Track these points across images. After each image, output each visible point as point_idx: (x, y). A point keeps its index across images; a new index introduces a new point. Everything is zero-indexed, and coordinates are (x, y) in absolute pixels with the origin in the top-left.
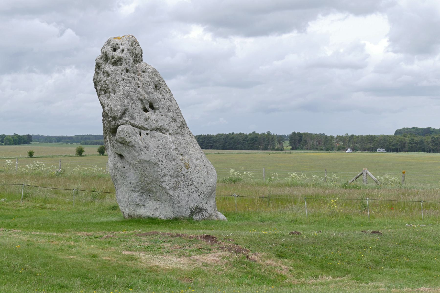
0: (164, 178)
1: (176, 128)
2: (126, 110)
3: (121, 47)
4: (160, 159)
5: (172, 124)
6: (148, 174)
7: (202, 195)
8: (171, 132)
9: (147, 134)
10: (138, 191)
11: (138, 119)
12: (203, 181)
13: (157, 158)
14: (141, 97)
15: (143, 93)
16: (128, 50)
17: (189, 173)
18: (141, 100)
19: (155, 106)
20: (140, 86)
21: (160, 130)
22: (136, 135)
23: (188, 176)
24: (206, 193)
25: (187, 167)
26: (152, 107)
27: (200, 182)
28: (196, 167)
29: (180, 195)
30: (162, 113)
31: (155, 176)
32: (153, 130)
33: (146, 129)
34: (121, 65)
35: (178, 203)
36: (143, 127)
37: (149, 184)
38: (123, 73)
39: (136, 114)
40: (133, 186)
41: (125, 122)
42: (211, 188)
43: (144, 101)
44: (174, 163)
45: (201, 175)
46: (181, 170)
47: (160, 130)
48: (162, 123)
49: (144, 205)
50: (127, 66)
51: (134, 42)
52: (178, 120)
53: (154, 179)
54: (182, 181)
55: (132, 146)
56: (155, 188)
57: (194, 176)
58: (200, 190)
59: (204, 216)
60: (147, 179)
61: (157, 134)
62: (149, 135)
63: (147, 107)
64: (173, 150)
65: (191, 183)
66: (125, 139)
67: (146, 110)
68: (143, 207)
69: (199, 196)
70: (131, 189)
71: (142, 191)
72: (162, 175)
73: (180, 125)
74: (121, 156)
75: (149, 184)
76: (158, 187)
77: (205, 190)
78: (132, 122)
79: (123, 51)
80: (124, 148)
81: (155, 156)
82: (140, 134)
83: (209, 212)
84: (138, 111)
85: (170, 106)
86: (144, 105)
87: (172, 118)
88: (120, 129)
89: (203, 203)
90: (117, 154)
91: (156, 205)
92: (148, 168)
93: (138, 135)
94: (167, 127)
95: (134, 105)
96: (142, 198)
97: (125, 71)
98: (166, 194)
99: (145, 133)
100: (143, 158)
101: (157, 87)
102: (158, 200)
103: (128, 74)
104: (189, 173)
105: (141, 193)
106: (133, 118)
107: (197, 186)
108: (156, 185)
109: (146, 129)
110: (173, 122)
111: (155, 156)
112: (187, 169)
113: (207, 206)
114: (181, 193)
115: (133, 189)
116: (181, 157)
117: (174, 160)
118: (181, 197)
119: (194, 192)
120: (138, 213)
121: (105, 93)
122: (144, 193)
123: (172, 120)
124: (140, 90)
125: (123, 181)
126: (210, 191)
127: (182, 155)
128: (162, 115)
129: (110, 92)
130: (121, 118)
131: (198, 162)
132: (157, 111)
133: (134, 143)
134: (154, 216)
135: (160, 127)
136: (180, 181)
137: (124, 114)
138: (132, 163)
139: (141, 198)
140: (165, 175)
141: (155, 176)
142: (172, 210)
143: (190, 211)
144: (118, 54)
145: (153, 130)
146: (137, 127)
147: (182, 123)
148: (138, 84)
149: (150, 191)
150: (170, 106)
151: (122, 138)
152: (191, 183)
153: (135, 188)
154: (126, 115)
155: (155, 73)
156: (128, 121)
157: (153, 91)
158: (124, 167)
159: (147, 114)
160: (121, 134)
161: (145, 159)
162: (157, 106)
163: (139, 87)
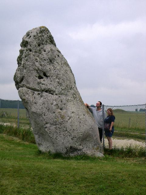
1: (61, 90)
2: (23, 77)
7: (75, 139)
9: (39, 94)
11: (32, 83)
12: (75, 128)
14: (37, 68)
17: (64, 122)
18: (37, 71)
21: (48, 91)
23: (63, 124)
24: (77, 137)
25: (63, 117)
26: (45, 75)
27: (72, 129)
32: (43, 91)
33: (38, 91)
39: (31, 79)
42: (82, 134)
43: (39, 71)
44: (54, 114)
45: (73, 124)
46: (58, 120)
47: (48, 91)
48: (50, 87)
51: (44, 31)
54: (59, 128)
57: (68, 125)
58: (72, 135)
63: (42, 75)
65: (65, 129)
67: (40, 77)
69: (72, 139)
71: (39, 134)
72: (44, 123)
77: (77, 135)
78: (28, 85)
79: (30, 37)
86: (39, 74)
89: (77, 145)
94: (53, 89)
95: (30, 73)
96: (40, 139)
101: (51, 61)
106: (28, 82)
107: (70, 132)
109: (38, 91)
113: (81, 147)
116: (60, 110)
117: (54, 113)
118: (59, 139)
123: (58, 84)
127: (61, 109)
131: (72, 115)
133: (27, 100)
135: (49, 89)
140: (47, 123)
145: (43, 91)
146: (31, 89)
147: (67, 87)
148: (36, 59)
150: (58, 75)
154: (23, 81)
156: (24, 85)
159: (42, 80)
162: (48, 75)
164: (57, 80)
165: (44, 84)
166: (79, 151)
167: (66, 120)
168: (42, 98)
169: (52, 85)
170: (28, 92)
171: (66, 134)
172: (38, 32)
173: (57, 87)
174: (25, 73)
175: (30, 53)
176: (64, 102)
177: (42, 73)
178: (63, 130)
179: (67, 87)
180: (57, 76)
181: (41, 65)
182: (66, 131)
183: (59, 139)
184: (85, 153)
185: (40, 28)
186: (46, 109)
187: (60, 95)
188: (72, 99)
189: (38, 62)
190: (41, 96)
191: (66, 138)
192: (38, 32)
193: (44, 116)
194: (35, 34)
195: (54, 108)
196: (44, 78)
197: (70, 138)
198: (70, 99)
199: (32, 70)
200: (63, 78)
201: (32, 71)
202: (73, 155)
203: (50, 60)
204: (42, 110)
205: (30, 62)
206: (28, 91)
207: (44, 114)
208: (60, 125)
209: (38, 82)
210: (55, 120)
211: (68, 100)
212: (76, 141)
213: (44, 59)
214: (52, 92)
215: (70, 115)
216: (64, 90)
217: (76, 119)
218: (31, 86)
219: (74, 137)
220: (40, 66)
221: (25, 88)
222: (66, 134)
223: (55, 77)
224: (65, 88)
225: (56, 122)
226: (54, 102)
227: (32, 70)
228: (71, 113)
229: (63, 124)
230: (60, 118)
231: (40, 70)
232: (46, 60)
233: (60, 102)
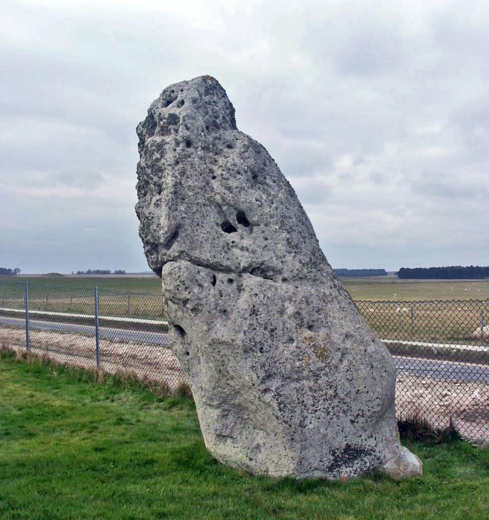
0: (268, 383)
1: (298, 265)
4: (258, 340)
5: (289, 258)
7: (361, 420)
9: (231, 281)
10: (218, 407)
11: (207, 246)
16: (194, 101)
17: (327, 369)
20: (215, 175)
24: (368, 414)
26: (243, 219)
27: (353, 390)
28: (343, 355)
29: (307, 422)
33: (228, 270)
36: (221, 266)
37: (238, 392)
40: (207, 395)
41: (177, 254)
42: (380, 402)
43: (225, 208)
45: (355, 375)
49: (231, 437)
50: (188, 133)
58: (354, 408)
59: (368, 464)
60: (232, 383)
62: (235, 284)
63: (233, 220)
64: (289, 318)
65: (331, 392)
67: (229, 228)
69: (352, 422)
70: (204, 400)
71: (226, 407)
73: (307, 259)
75: (238, 392)
77: (366, 408)
78: (196, 254)
79: (182, 103)
81: (245, 332)
83: (378, 455)
85: (286, 217)
86: (225, 216)
87: (289, 243)
88: (166, 269)
89: (363, 437)
94: (276, 263)
98: (274, 418)
99: (225, 279)
100: (219, 335)
104: (327, 369)
107: (348, 400)
108: (253, 398)
109: (228, 270)
110: (290, 253)
111: (245, 332)
113: (372, 442)
115: (208, 403)
116: (308, 333)
117: (291, 340)
119: (341, 414)
120: (221, 452)
122: (230, 411)
124: (215, 184)
126: (379, 408)
127: (310, 328)
128: (266, 239)
130: (168, 245)
131: (348, 344)
132: (255, 229)
134: (253, 463)
135: (262, 264)
136: (307, 389)
139: (224, 421)
141: (247, 378)
145: (245, 270)
146: (207, 266)
147: (314, 255)
148: (211, 171)
149: (240, 408)
150: (286, 217)
151: (169, 291)
152: (331, 392)
153: (211, 399)
155: (257, 148)
158: (188, 354)
161: (224, 339)
162: (255, 219)
163: (214, 178)
164: (285, 235)
165: (247, 250)
166: (366, 456)
167: (333, 361)
168: (245, 296)
169: (269, 250)
170: (198, 277)
171: (333, 408)
172: (202, 90)
173: (284, 256)
174: (184, 215)
175: (191, 150)
176: (316, 303)
177: (235, 213)
178: (326, 394)
179: (314, 255)
180: (282, 222)
181: (229, 189)
182: (335, 397)
183: (311, 426)
184: (382, 458)
185: (205, 79)
186: (266, 329)
187: (297, 283)
188: (335, 292)
189: (219, 178)
190: (240, 289)
191: (335, 419)
192: (200, 89)
193: (259, 354)
194: (196, 95)
195: (291, 324)
196: (240, 231)
197: (346, 420)
198: (327, 292)
199: (204, 205)
200: (300, 230)
201: (203, 209)
202: (351, 469)
203: (253, 172)
204: (252, 335)
205: (195, 178)
206: (199, 272)
207: (259, 346)
208: (316, 381)
209: (228, 244)
210: (298, 364)
211: (324, 298)
212: (363, 428)
213: (236, 169)
214: (270, 273)
215: (342, 346)
216: (308, 265)
217: (359, 356)
218: (205, 255)
219: (358, 414)
220: (226, 191)
221: (184, 263)
223: (277, 227)
224: (311, 259)
225: (300, 370)
226: (287, 304)
227: (204, 205)
228: (342, 338)
230: (314, 357)
231: (228, 204)
232: (242, 172)
233: (303, 306)
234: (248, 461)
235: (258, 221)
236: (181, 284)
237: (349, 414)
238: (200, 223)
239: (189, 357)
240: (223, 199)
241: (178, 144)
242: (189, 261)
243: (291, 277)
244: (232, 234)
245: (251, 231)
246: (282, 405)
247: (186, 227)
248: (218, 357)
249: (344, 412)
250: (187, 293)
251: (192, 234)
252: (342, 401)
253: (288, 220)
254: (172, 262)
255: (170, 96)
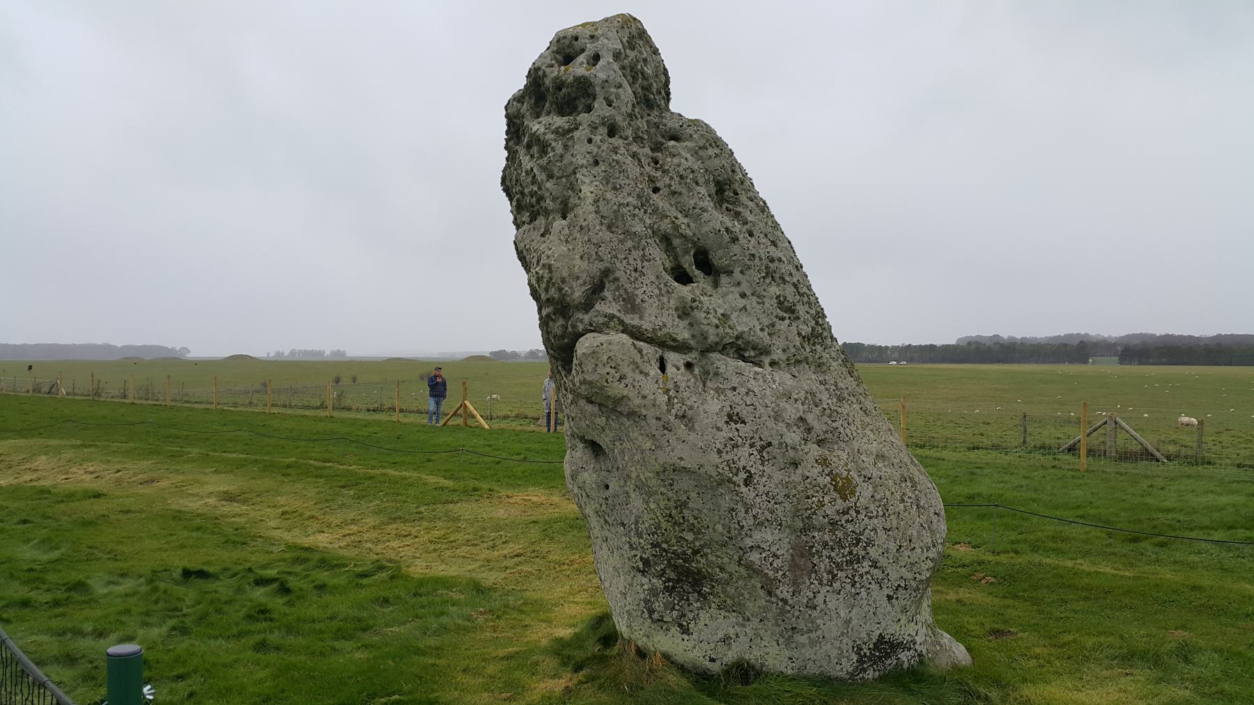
0: (758, 536)
1: (798, 341)
2: (606, 273)
3: (591, 48)
6: (696, 518)
8: (778, 355)
11: (651, 308)
13: (729, 457)
15: (673, 212)
16: (617, 56)
18: (666, 240)
19: (718, 258)
22: (647, 368)
23: (850, 527)
26: (705, 263)
30: (745, 287)
31: (719, 527)
33: (682, 348)
34: (589, 109)
35: (810, 631)
36: (675, 340)
38: (597, 138)
39: (645, 289)
41: (601, 320)
43: (676, 242)
46: (821, 504)
47: (741, 349)
48: (746, 325)
50: (608, 112)
52: (801, 309)
53: (717, 537)
54: (825, 544)
55: (632, 414)
56: (722, 569)
58: (894, 576)
60: (689, 536)
61: (727, 364)
63: (688, 262)
66: (602, 388)
67: (683, 278)
68: (675, 630)
69: (890, 598)
74: (595, 449)
76: (733, 567)
77: (910, 576)
79: (596, 58)
80: (601, 421)
82: (663, 368)
84: (653, 278)
85: (772, 260)
86: (676, 258)
87: (780, 303)
90: (582, 439)
91: (724, 624)
92: (693, 495)
93: (654, 370)
97: (603, 130)
99: (681, 364)
100: (673, 458)
102: (733, 607)
103: (616, 141)
105: (669, 580)
106: (631, 304)
107: (883, 561)
108: (726, 560)
110: (783, 319)
111: (719, 452)
112: (845, 499)
113: (911, 629)
114: (824, 590)
119: (874, 586)
121: (533, 218)
123: (781, 314)
125: (607, 534)
129: (547, 213)
130: (587, 306)
132: (724, 279)
133: (637, 401)
135: (738, 338)
137: (597, 290)
138: (634, 475)
141: (719, 527)
142: (787, 653)
143: (855, 658)
144: (579, 68)
146: (650, 341)
147: (817, 323)
150: (772, 260)
154: (606, 293)
156: (612, 317)
157: (708, 204)
158: (607, 487)
159: (685, 291)
160: (589, 367)
163: (656, 190)
171: (861, 576)
173: (773, 325)
178: (850, 553)
186: (752, 446)
189: (664, 191)
195: (793, 437)
203: (717, 183)
207: (743, 475)
222: (861, 576)
229: (847, 521)
234: (707, 663)
235: (729, 265)
236: (613, 371)
237: (884, 587)
238: (639, 268)
239: (608, 493)
240: (676, 227)
241: (594, 128)
242: (623, 332)
243: (784, 358)
244: (688, 288)
245: (716, 285)
246: (781, 573)
247: (618, 274)
248: (670, 494)
249: (879, 583)
250: (623, 385)
251: (628, 286)
252: (875, 565)
253: (776, 264)
254: (595, 334)
255: (570, 46)
